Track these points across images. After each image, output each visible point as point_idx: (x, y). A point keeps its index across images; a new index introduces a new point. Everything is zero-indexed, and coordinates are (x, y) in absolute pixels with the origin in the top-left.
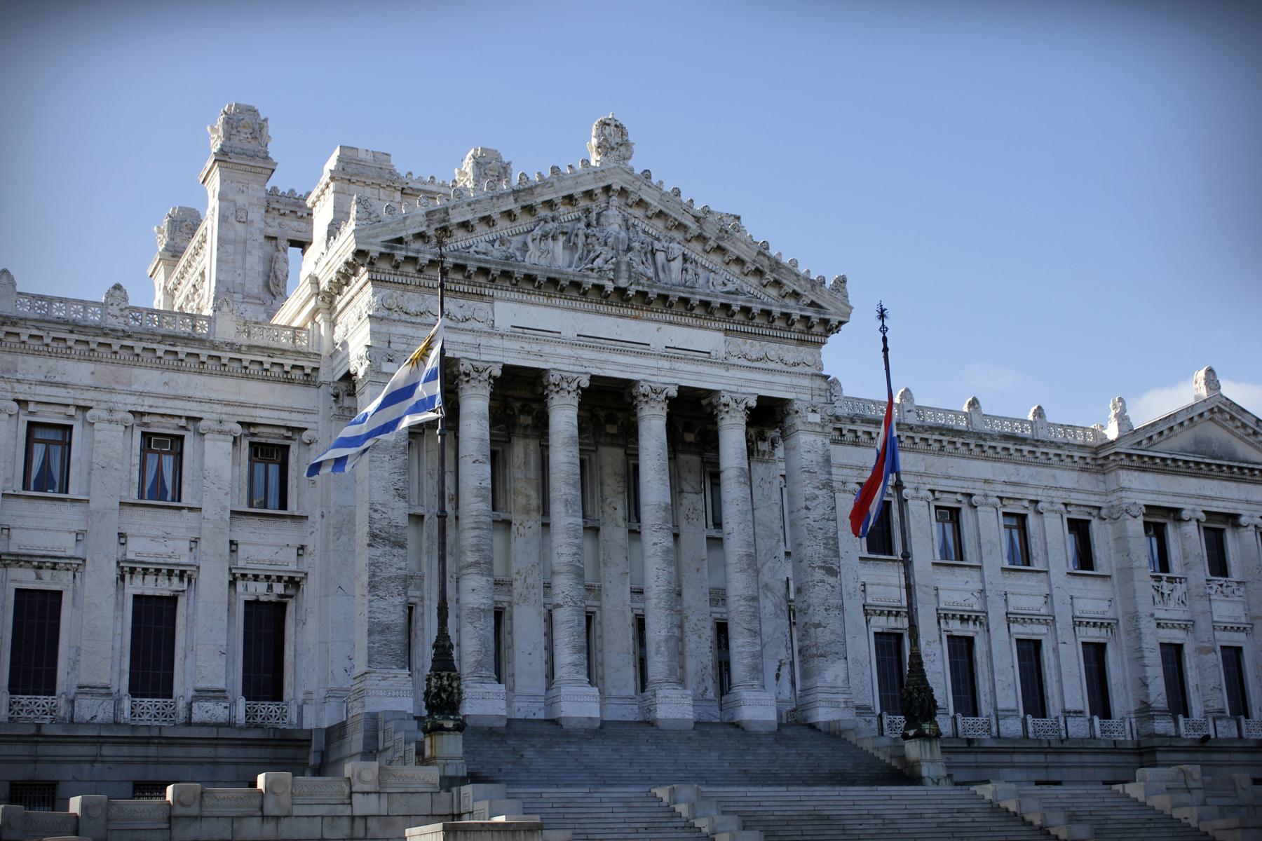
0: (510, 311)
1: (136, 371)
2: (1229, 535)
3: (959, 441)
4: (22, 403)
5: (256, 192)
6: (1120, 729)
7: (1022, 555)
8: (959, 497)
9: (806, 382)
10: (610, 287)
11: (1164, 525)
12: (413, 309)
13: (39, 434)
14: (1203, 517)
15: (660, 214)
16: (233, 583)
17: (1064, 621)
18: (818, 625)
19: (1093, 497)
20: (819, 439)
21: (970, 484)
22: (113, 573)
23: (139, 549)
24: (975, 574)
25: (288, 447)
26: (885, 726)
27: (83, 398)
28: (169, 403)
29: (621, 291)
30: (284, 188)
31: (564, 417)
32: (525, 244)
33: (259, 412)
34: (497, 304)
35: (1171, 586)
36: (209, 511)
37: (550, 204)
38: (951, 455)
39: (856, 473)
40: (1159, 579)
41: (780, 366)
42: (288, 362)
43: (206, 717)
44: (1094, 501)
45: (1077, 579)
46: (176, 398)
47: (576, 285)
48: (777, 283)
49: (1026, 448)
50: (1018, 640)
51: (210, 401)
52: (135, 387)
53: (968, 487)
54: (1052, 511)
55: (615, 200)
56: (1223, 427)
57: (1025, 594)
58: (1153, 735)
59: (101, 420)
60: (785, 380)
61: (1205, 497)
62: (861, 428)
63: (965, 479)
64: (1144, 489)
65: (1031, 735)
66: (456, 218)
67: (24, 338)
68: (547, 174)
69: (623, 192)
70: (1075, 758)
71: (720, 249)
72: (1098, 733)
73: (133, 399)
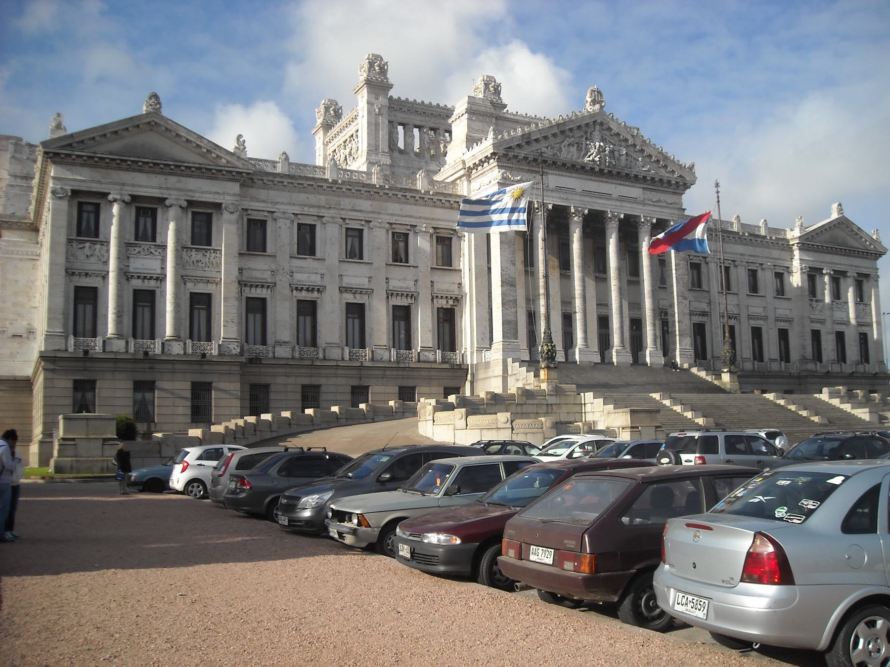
1: (389, 204)
2: (842, 280)
4: (344, 219)
5: (382, 101)
7: (754, 288)
9: (676, 212)
10: (597, 169)
13: (350, 233)
16: (432, 300)
17: (772, 318)
22: (385, 296)
23: (394, 284)
24: (735, 296)
25: (451, 238)
27: (368, 217)
28: (404, 219)
29: (601, 170)
30: (395, 97)
32: (561, 148)
33: (440, 222)
34: (550, 177)
36: (422, 267)
37: (571, 130)
40: (812, 300)
41: (665, 204)
42: (452, 200)
43: (425, 359)
45: (777, 300)
46: (406, 216)
51: (420, 218)
52: (390, 212)
53: (734, 257)
55: (598, 127)
57: (756, 306)
58: (807, 370)
59: (376, 227)
60: (667, 211)
66: (534, 138)
67: (344, 190)
69: (601, 124)
70: (773, 380)
73: (388, 217)
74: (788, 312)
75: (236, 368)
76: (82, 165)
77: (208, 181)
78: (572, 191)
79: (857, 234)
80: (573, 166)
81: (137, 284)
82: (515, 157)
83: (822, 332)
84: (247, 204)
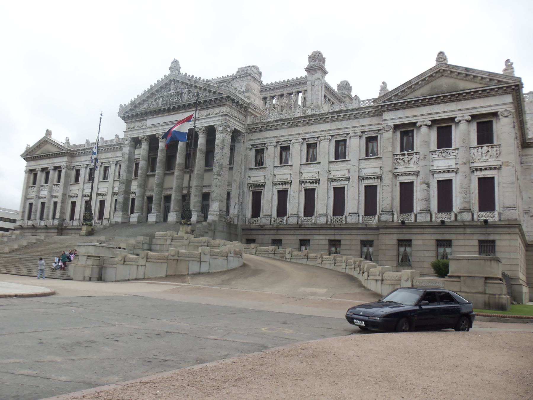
0: (150, 122)
3: (313, 119)
6: (373, 219)
8: (316, 139)
9: (220, 118)
11: (413, 131)
12: (132, 126)
14: (430, 123)
15: (182, 83)
18: (213, 192)
19: (377, 126)
20: (221, 135)
21: (319, 133)
26: (272, 221)
31: (162, 145)
34: (148, 121)
35: (410, 157)
37: (157, 91)
38: (312, 124)
39: (275, 139)
41: (215, 115)
44: (377, 127)
47: (160, 110)
48: (210, 91)
49: (342, 115)
50: (334, 188)
54: (355, 136)
56: (451, 77)
57: (339, 170)
60: (214, 119)
61: (431, 114)
62: (275, 124)
63: (317, 132)
64: (393, 118)
65: (329, 223)
68: (156, 83)
69: (174, 80)
70: (348, 232)
71: (196, 87)
72: (361, 221)
74: (377, 170)
75: (56, 231)
76: (32, 160)
77: (59, 158)
78: (158, 125)
79: (467, 75)
80: (155, 111)
81: (42, 200)
82: (128, 116)
83: (415, 184)
84: (74, 164)
